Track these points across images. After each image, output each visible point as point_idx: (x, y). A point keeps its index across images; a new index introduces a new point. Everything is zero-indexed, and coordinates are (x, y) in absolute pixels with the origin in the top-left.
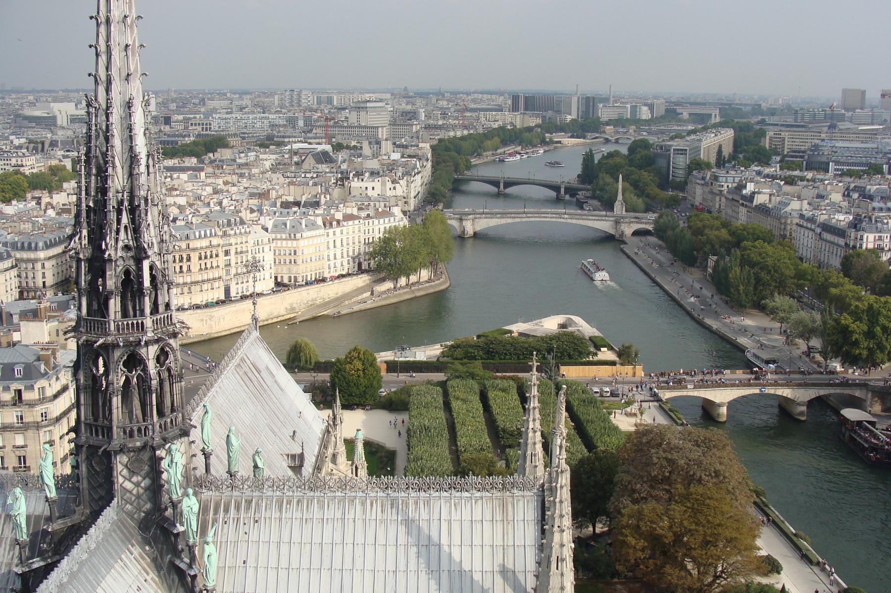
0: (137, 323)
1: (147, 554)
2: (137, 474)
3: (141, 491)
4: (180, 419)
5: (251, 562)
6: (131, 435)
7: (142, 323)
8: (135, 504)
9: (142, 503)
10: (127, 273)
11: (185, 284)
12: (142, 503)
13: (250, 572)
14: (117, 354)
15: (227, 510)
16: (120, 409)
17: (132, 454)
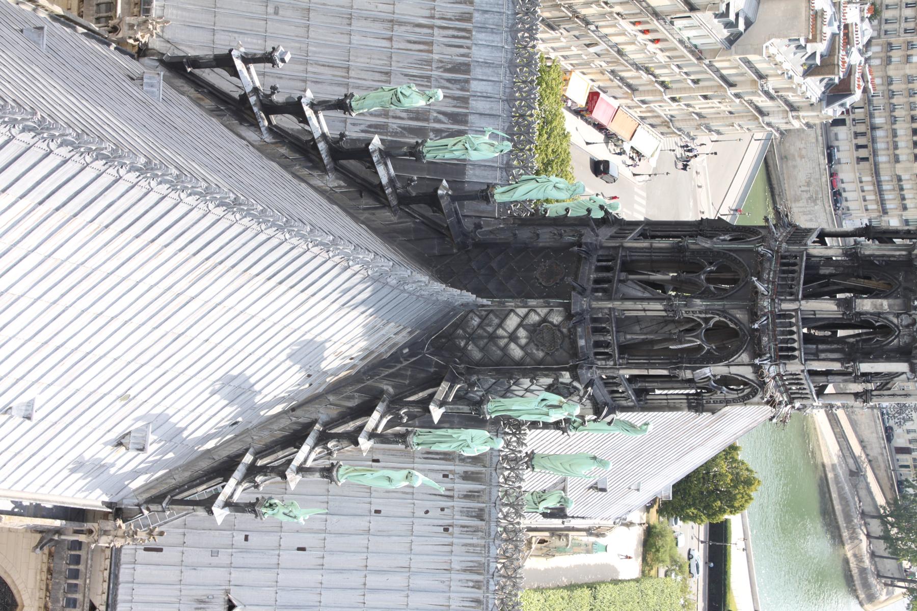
0: (794, 349)
1: (396, 352)
2: (530, 339)
3: (502, 343)
4: (624, 403)
5: (377, 522)
6: (596, 330)
7: (794, 357)
8: (480, 331)
9: (482, 343)
10: (886, 330)
11: (875, 153)
12: (482, 343)
13: (362, 523)
14: (740, 315)
15: (466, 477)
16: (642, 313)
17: (565, 330)
